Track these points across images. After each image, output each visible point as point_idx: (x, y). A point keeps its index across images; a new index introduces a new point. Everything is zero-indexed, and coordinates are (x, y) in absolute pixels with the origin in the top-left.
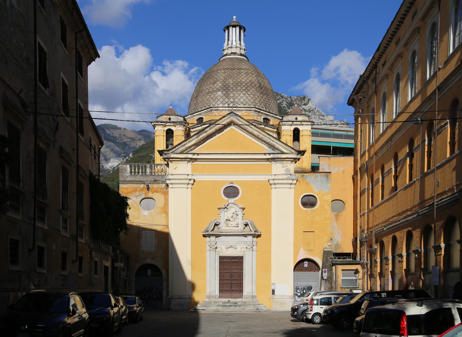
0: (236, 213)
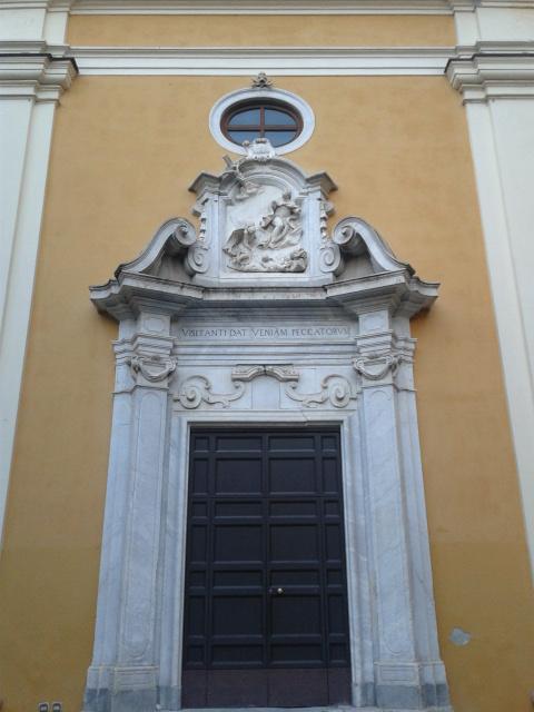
0: (291, 204)
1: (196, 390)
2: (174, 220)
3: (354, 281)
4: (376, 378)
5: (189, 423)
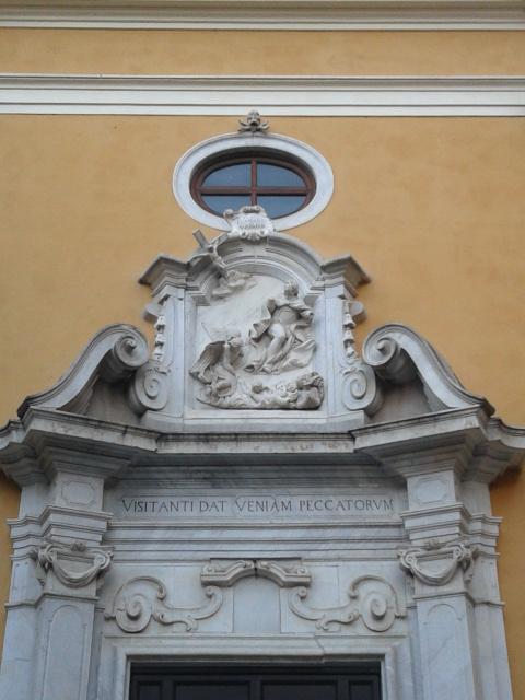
0: (298, 303)
1: (142, 600)
2: (115, 328)
3: (399, 424)
4: (437, 582)
5: (129, 657)
